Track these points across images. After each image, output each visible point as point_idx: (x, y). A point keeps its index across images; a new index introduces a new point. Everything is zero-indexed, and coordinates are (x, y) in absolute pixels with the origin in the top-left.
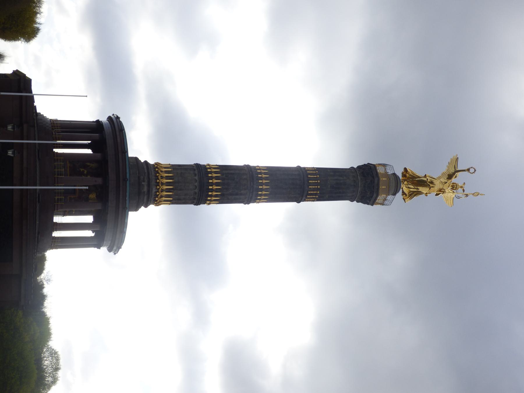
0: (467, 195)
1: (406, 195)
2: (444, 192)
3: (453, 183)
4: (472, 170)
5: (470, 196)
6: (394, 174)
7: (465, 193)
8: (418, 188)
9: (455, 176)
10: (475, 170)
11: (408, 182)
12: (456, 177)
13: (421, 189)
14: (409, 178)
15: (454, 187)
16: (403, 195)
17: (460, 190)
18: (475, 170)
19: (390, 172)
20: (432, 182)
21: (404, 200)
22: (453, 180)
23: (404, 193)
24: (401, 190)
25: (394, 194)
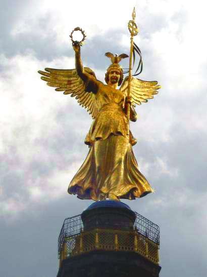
0: (135, 49)
1: (134, 189)
2: (128, 101)
3: (107, 79)
4: (78, 37)
5: (137, 40)
6: (85, 216)
7: (127, 51)
8: (117, 160)
9: (90, 76)
10: (77, 29)
11: (102, 185)
12: (92, 74)
13: (120, 156)
14: (93, 181)
15: (115, 77)
16: (134, 198)
17: (123, 65)
18: (77, 29)
19: (78, 227)
20: (106, 128)
21: (145, 194)
22: (100, 76)
23: (130, 195)
24: (122, 200)
25: (132, 216)
